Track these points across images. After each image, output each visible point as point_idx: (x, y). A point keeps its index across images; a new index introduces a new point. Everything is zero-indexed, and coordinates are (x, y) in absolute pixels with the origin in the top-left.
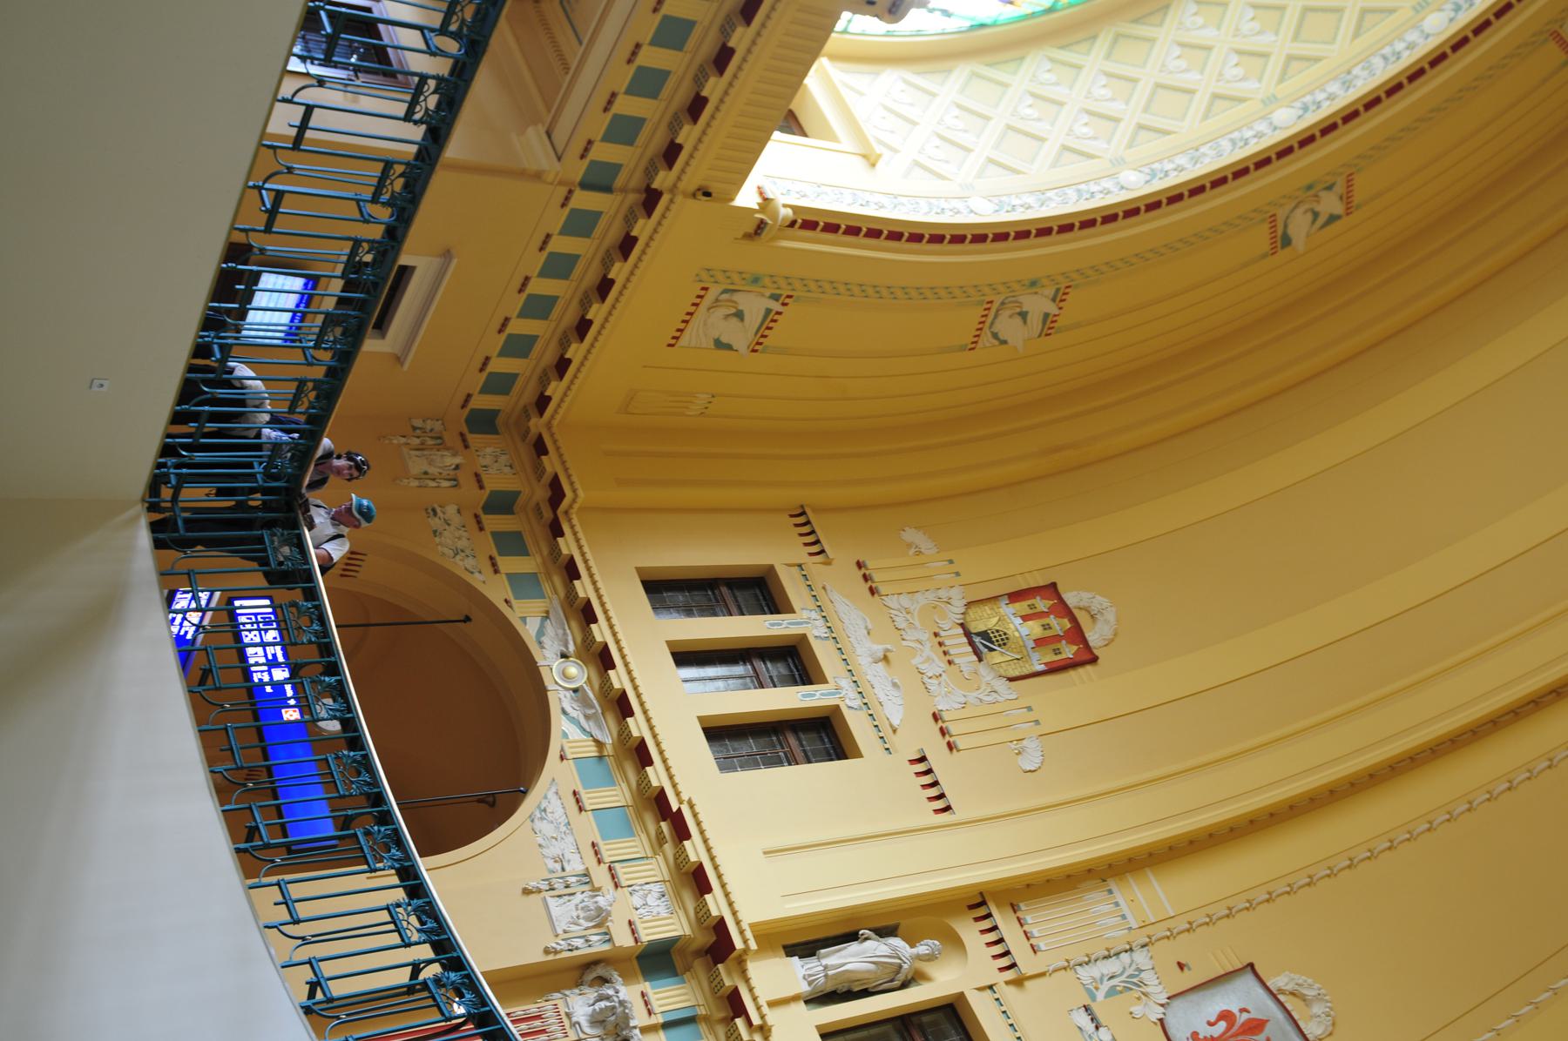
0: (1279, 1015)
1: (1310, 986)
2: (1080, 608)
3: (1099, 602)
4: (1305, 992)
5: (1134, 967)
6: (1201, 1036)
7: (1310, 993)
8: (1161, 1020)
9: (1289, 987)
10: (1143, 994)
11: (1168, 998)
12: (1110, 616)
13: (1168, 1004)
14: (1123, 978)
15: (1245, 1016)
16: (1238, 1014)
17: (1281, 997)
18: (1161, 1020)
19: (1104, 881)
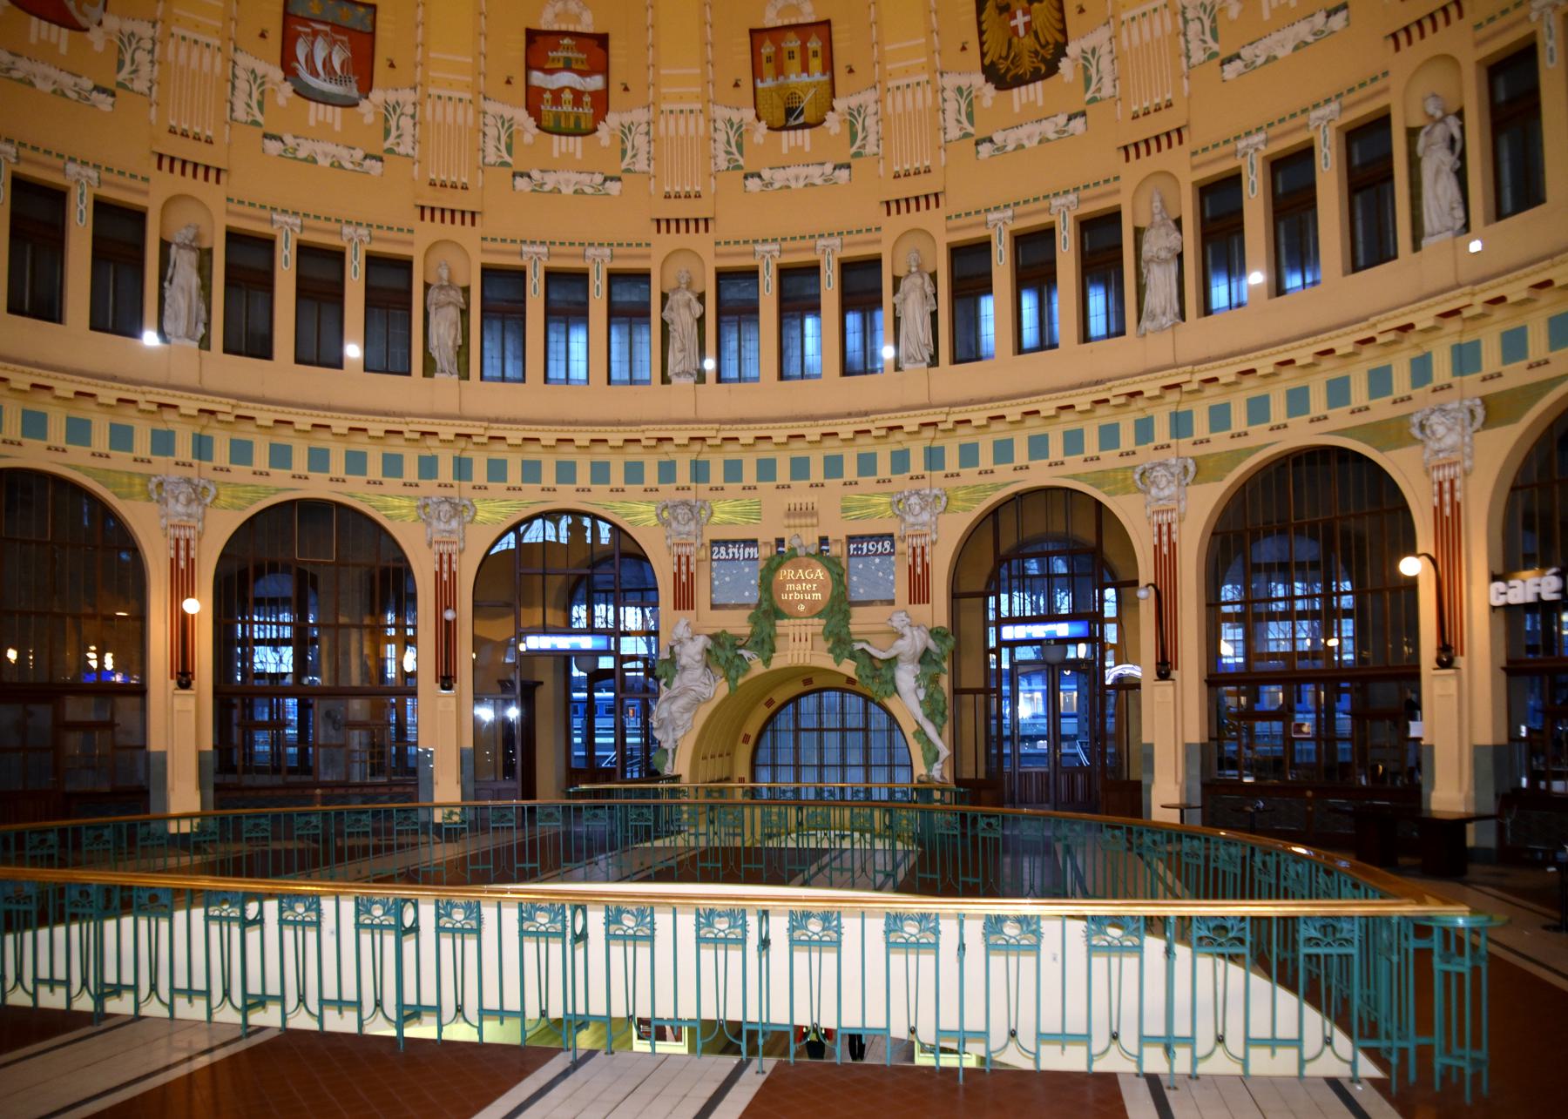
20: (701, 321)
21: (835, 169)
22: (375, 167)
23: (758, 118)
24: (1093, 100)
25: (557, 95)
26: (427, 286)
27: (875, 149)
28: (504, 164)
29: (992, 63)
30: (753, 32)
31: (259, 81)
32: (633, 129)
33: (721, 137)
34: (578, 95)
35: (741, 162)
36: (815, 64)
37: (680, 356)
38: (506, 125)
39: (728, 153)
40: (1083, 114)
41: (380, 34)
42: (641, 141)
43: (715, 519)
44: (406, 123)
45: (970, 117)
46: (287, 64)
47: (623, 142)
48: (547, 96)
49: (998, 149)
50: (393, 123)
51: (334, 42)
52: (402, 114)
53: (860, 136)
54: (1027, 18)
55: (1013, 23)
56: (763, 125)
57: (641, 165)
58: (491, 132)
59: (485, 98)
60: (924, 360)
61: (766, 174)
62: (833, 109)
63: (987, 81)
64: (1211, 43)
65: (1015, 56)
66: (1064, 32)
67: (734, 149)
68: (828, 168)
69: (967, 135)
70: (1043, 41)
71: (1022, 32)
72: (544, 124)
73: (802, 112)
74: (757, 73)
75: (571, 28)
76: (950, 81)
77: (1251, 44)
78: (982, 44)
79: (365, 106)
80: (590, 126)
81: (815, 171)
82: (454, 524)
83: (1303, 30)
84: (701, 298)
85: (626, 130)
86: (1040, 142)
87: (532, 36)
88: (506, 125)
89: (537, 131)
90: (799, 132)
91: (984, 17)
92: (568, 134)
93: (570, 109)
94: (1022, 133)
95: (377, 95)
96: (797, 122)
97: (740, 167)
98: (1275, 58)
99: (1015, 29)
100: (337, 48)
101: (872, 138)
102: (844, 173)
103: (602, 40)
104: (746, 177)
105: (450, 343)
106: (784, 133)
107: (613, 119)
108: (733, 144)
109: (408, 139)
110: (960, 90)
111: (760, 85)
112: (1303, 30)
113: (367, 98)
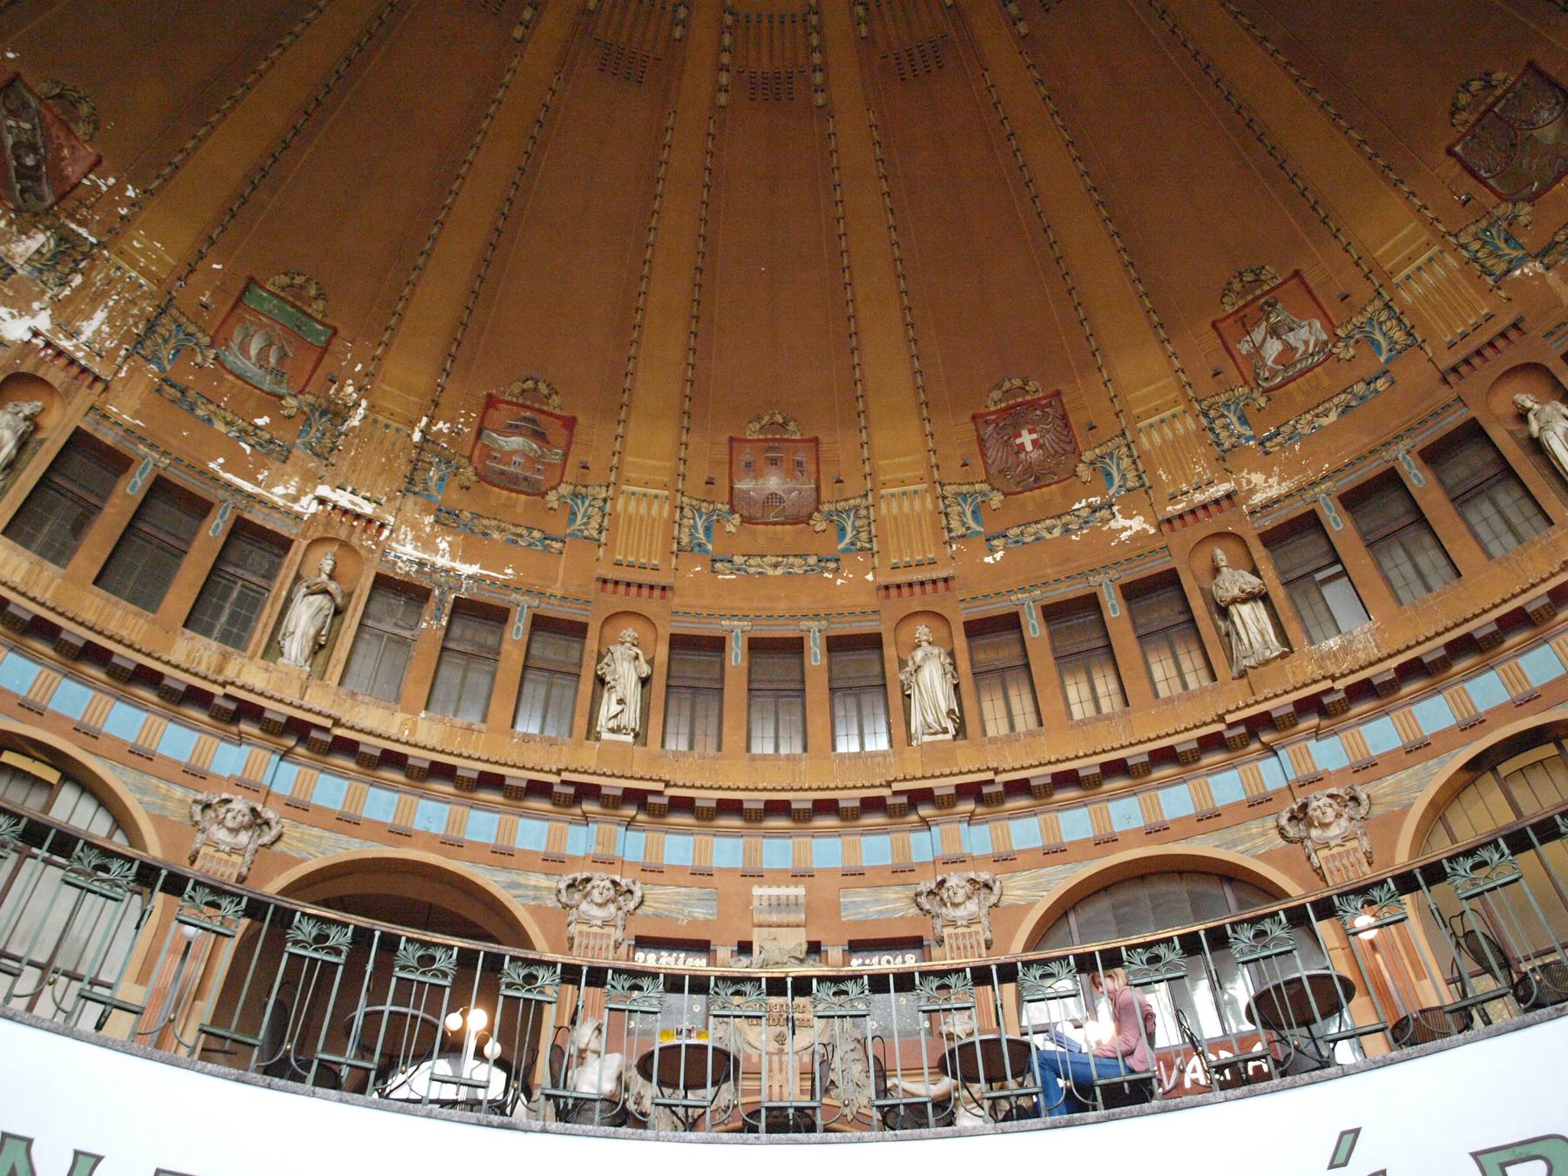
20: (645, 682)
23: (733, 511)
26: (298, 578)
35: (710, 547)
37: (615, 708)
43: (644, 909)
54: (1035, 436)
55: (1018, 441)
56: (737, 518)
60: (945, 731)
71: (1029, 447)
81: (798, 565)
82: (244, 838)
84: (650, 662)
99: (1022, 447)
104: (714, 561)
105: (312, 632)
111: (737, 486)
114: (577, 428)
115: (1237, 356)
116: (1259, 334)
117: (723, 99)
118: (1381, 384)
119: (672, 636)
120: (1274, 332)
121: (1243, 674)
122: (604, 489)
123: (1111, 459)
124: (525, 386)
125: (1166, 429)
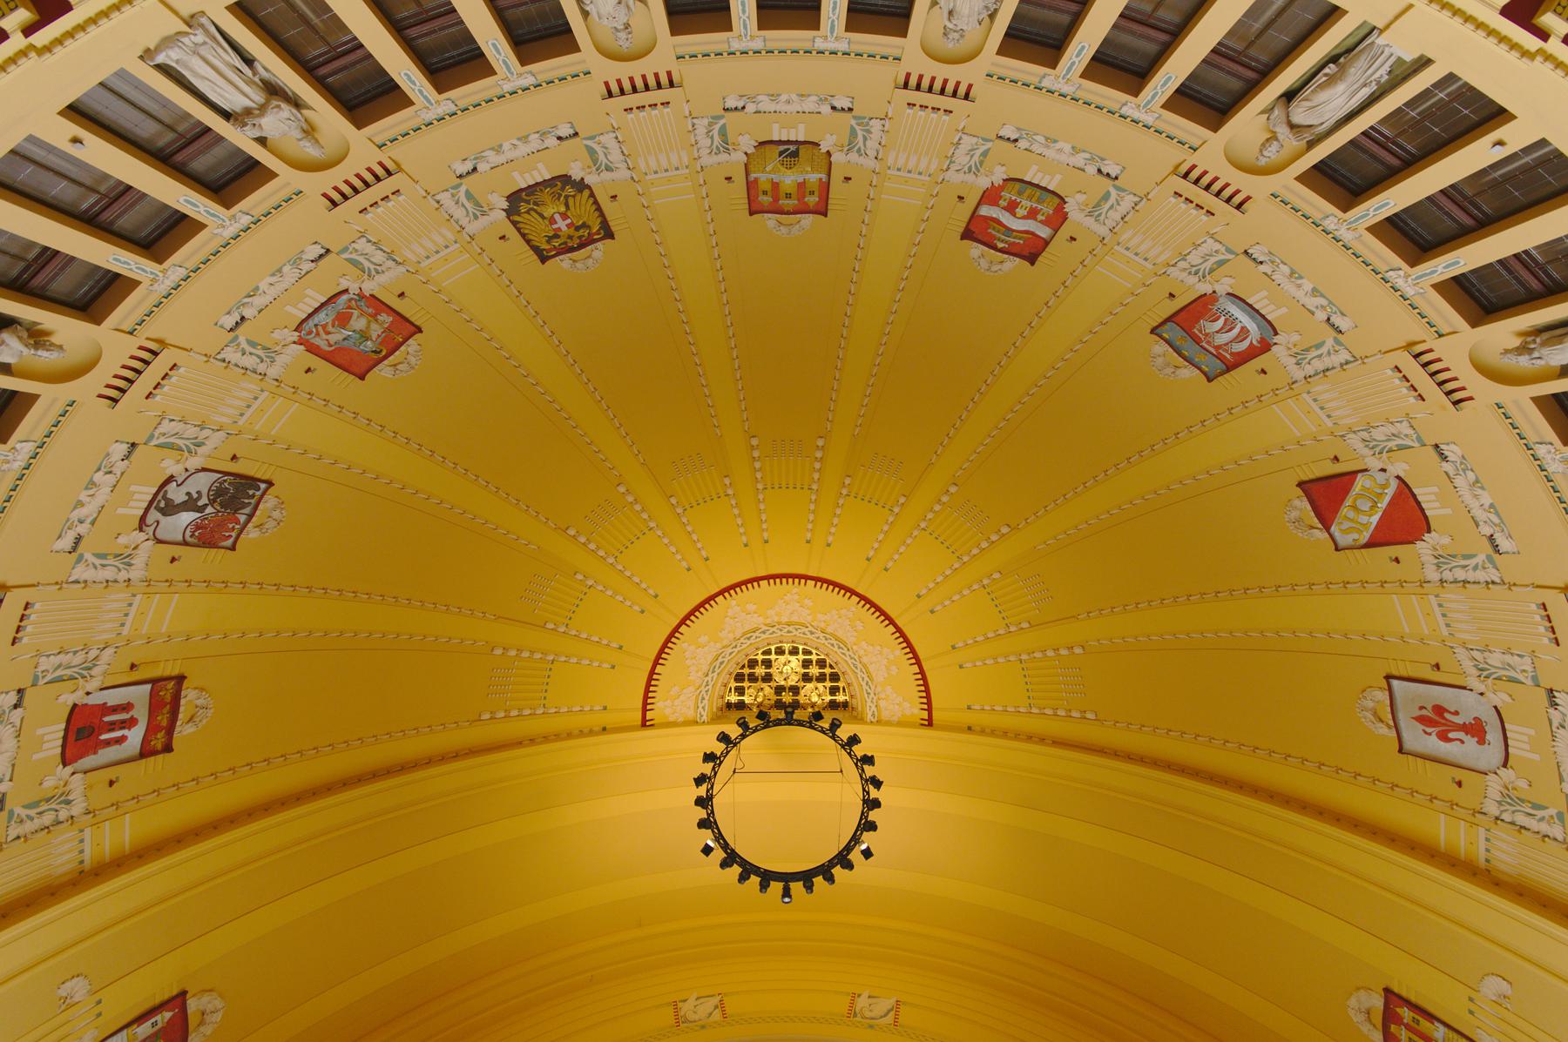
0: (1401, 716)
1: (1365, 718)
2: (1374, 1026)
3: (1358, 1018)
4: (1372, 717)
5: (1502, 808)
6: (1476, 739)
7: (1369, 715)
8: (1505, 765)
9: (1381, 725)
10: (1509, 790)
11: (1486, 774)
12: (1353, 1002)
13: (1490, 771)
14: (1519, 808)
15: (1429, 730)
16: (1434, 734)
17: (1391, 723)
18: (1505, 765)
19: (1487, 870)
21: (744, 108)
22: (1256, 252)
23: (829, 154)
24: (457, 187)
25: (1032, 214)
27: (695, 121)
28: (1118, 188)
29: (581, 191)
30: (825, 215)
31: (1299, 357)
32: (966, 169)
33: (872, 145)
34: (1011, 208)
35: (853, 122)
36: (764, 184)
38: (1097, 213)
39: (869, 132)
40: (460, 176)
41: (1165, 316)
42: (962, 159)
44: (1195, 258)
45: (591, 151)
46: (1265, 347)
47: (981, 163)
48: (1040, 217)
49: (550, 132)
50: (1208, 265)
51: (1207, 335)
52: (1192, 266)
53: (715, 133)
54: (555, 226)
55: (569, 221)
57: (968, 142)
58: (1115, 216)
59: (1103, 238)
61: (826, 109)
62: (746, 153)
63: (582, 179)
64: (354, 256)
65: (559, 199)
66: (514, 223)
67: (860, 134)
68: (751, 108)
69: (592, 138)
70: (533, 213)
71: (557, 217)
72: (1057, 201)
73: (781, 153)
74: (825, 188)
75: (993, 251)
76: (623, 174)
77: (307, 273)
78: (596, 202)
79: (1222, 289)
80: (1011, 184)
81: (766, 105)
83: (259, 301)
85: (974, 170)
86: (501, 146)
87: (1032, 259)
88: (1097, 213)
89: (1066, 199)
90: (784, 138)
91: (599, 220)
92: (1037, 186)
93: (1024, 202)
94: (524, 149)
95: (1205, 288)
96: (786, 147)
97: (855, 117)
98: (273, 275)
99: (564, 216)
100: (1207, 331)
101: (701, 130)
102: (730, 104)
103: (967, 235)
104: (850, 110)
106: (801, 139)
107: (984, 183)
108: (860, 138)
109: (1204, 249)
110: (608, 169)
111: (824, 177)
112: (259, 301)
113: (1214, 292)
114: (961, 230)
115: (386, 309)
116: (376, 330)
117: (820, 443)
118: (229, 322)
119: (903, 33)
120: (364, 336)
121: (191, 21)
122: (946, 179)
123: (474, 214)
124: (999, 267)
125: (429, 245)
